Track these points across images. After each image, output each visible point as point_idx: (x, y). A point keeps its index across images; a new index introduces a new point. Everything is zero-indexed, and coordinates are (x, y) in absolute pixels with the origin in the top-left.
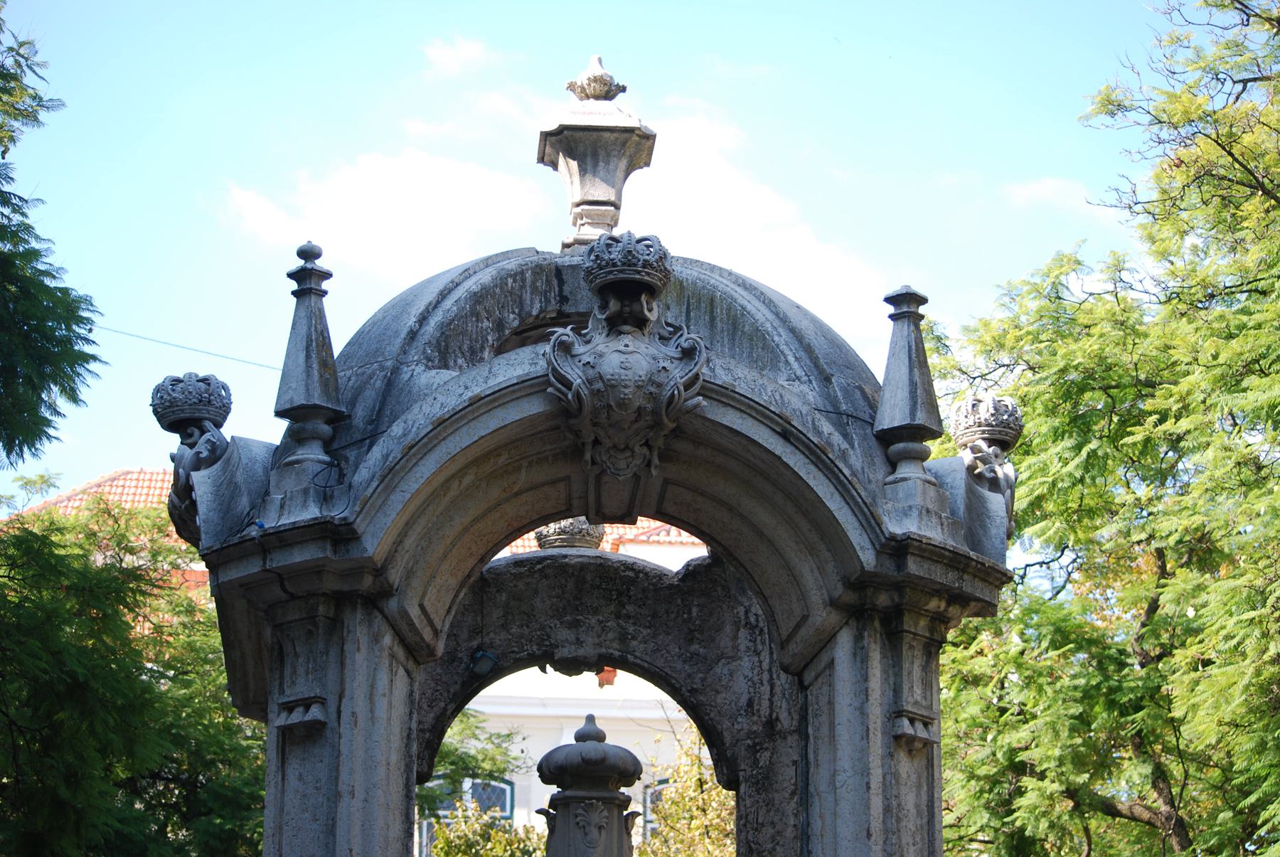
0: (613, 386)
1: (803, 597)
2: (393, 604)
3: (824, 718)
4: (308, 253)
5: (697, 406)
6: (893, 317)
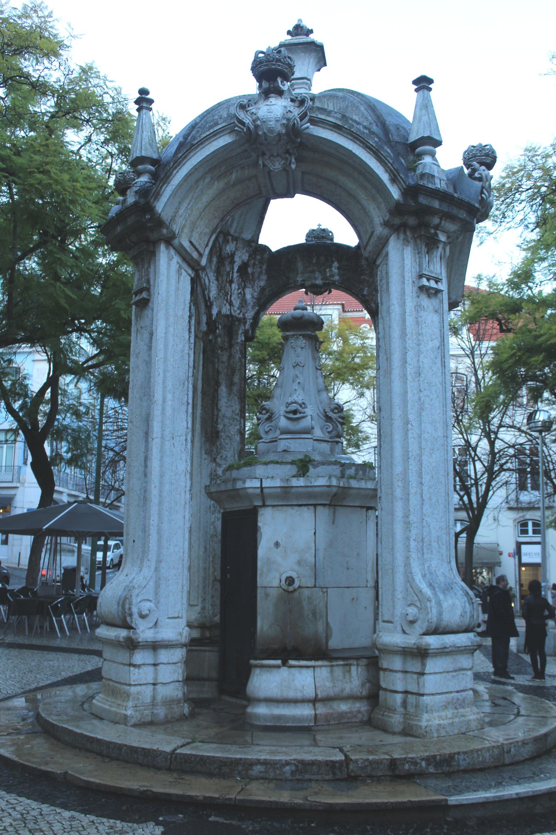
0: (264, 122)
1: (371, 222)
2: (176, 242)
3: (384, 281)
4: (143, 92)
5: (307, 128)
6: (416, 90)
